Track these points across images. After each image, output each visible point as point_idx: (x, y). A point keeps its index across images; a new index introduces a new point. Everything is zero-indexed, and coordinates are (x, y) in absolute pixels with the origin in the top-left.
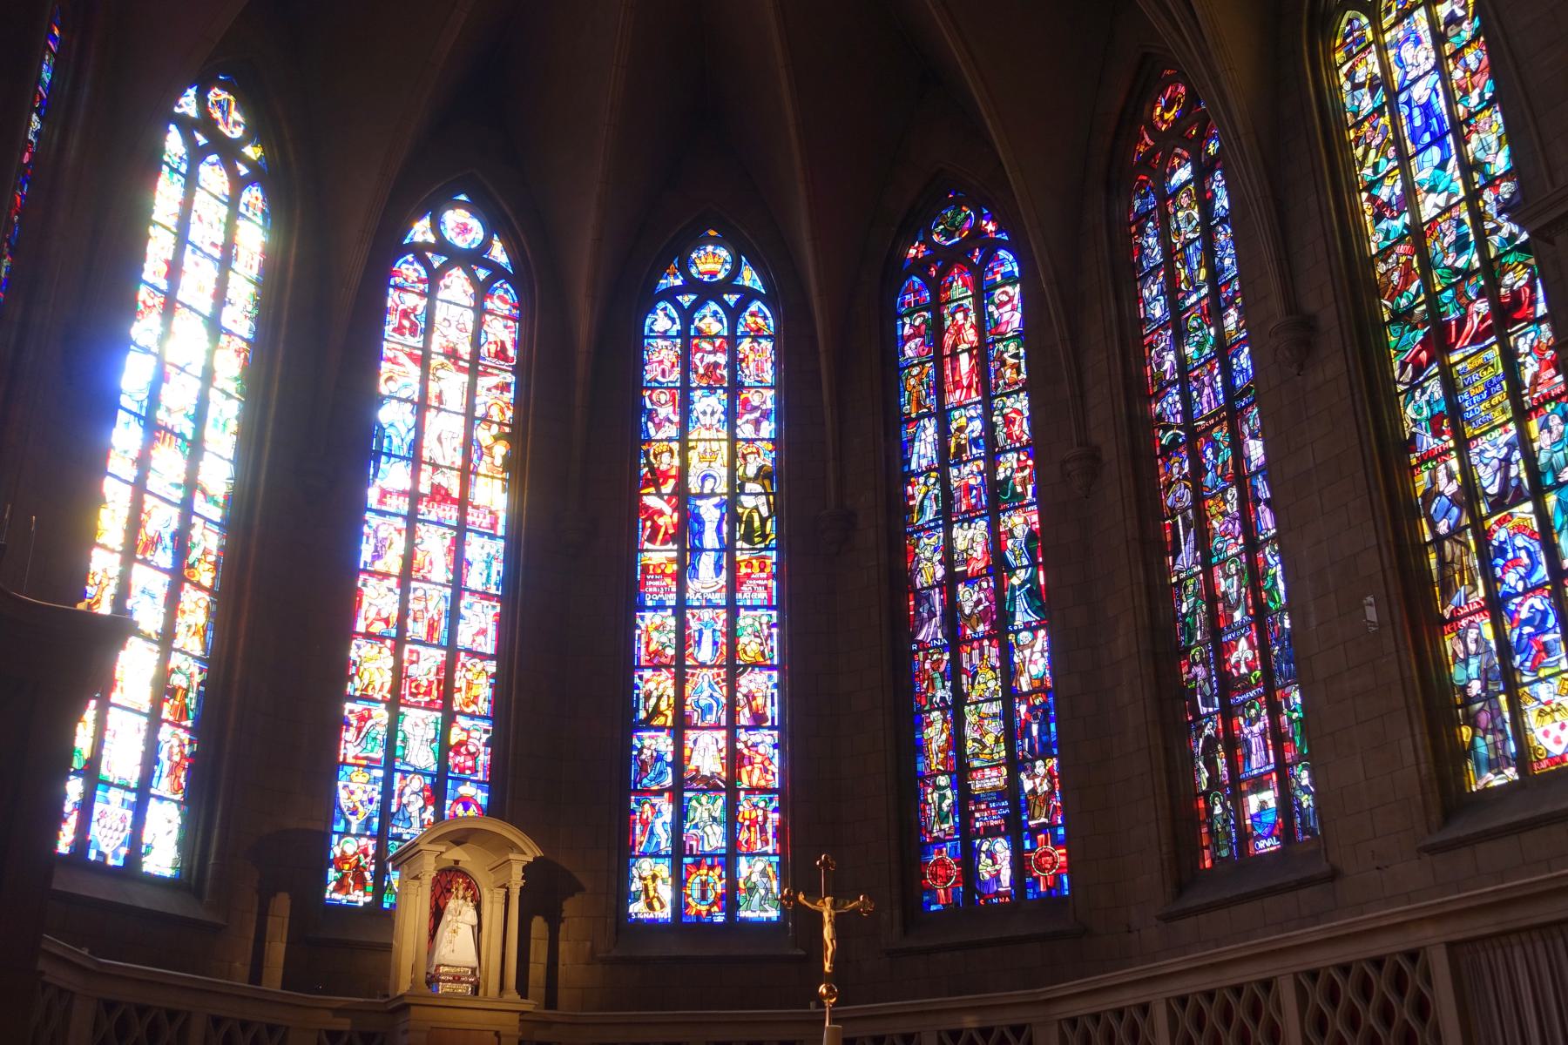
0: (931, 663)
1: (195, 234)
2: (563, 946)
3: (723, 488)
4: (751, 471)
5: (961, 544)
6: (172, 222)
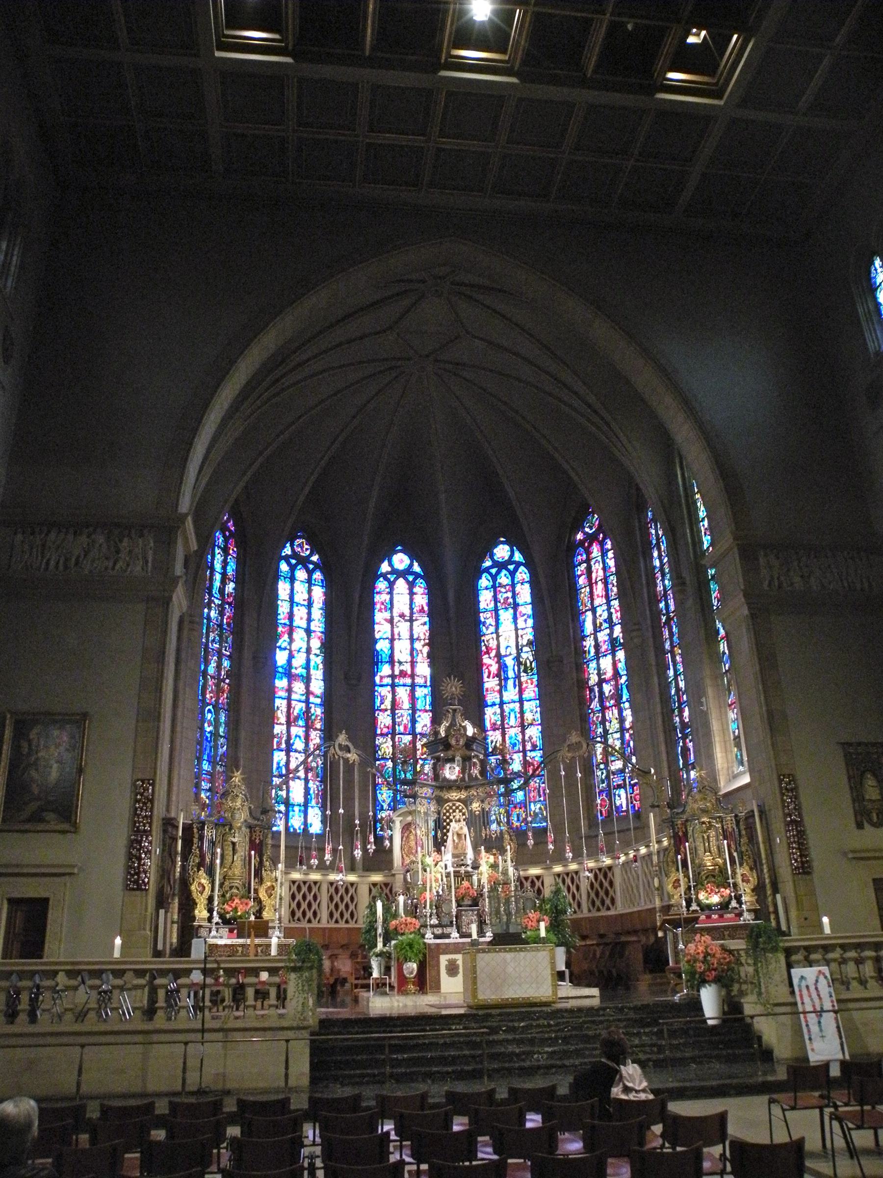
0: (596, 717)
1: (297, 599)
3: (514, 652)
4: (525, 643)
5: (602, 667)
6: (287, 598)
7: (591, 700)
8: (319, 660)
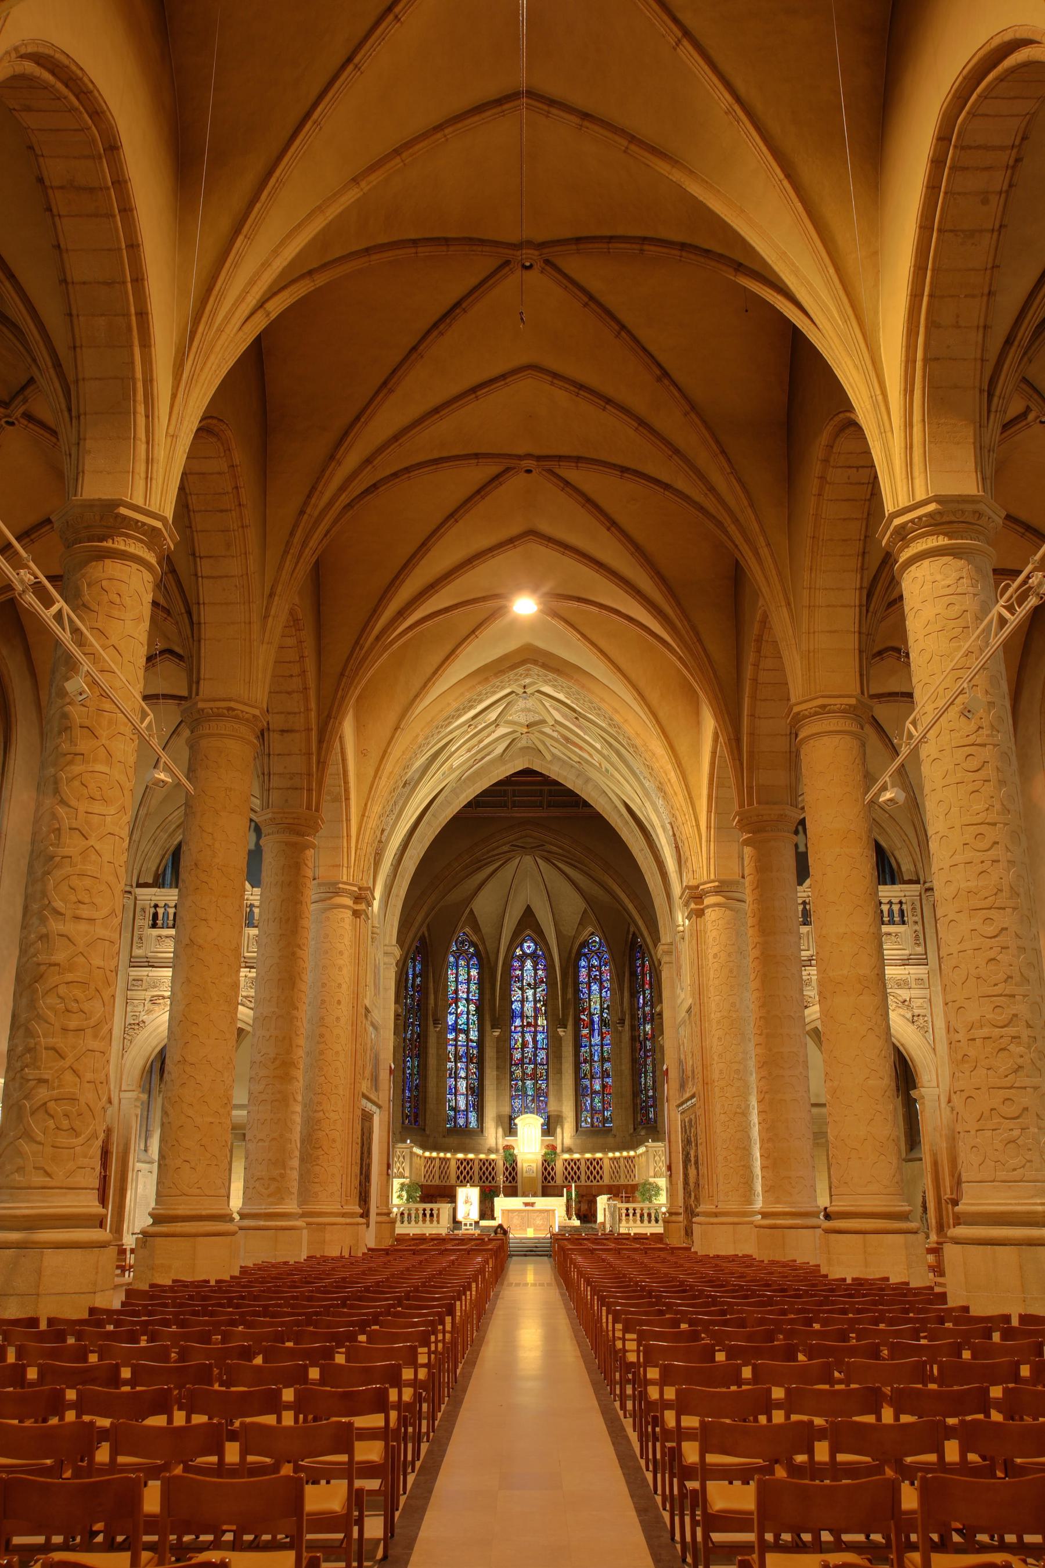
1: (460, 979)
2: (565, 1135)
4: (605, 1006)
7: (640, 1050)
8: (475, 1018)
